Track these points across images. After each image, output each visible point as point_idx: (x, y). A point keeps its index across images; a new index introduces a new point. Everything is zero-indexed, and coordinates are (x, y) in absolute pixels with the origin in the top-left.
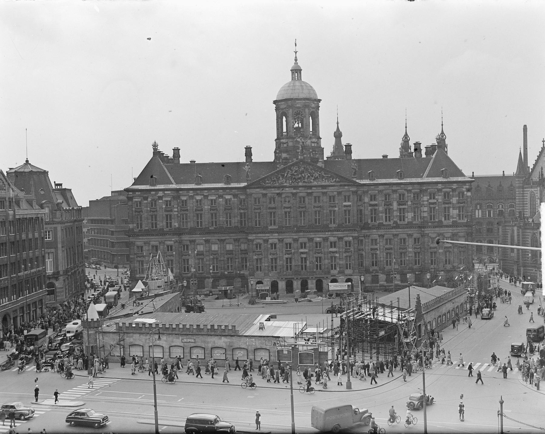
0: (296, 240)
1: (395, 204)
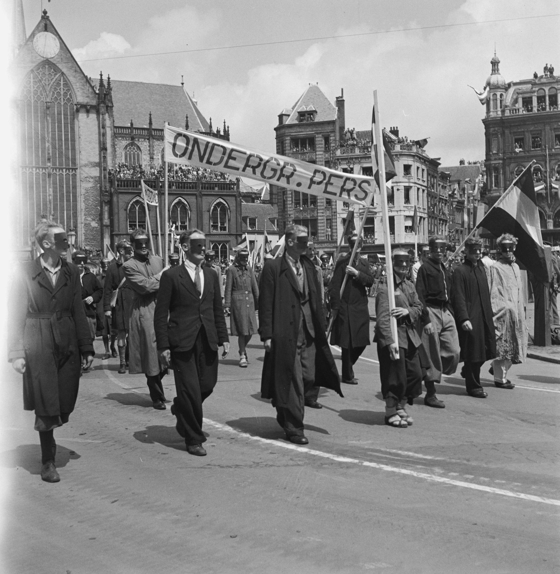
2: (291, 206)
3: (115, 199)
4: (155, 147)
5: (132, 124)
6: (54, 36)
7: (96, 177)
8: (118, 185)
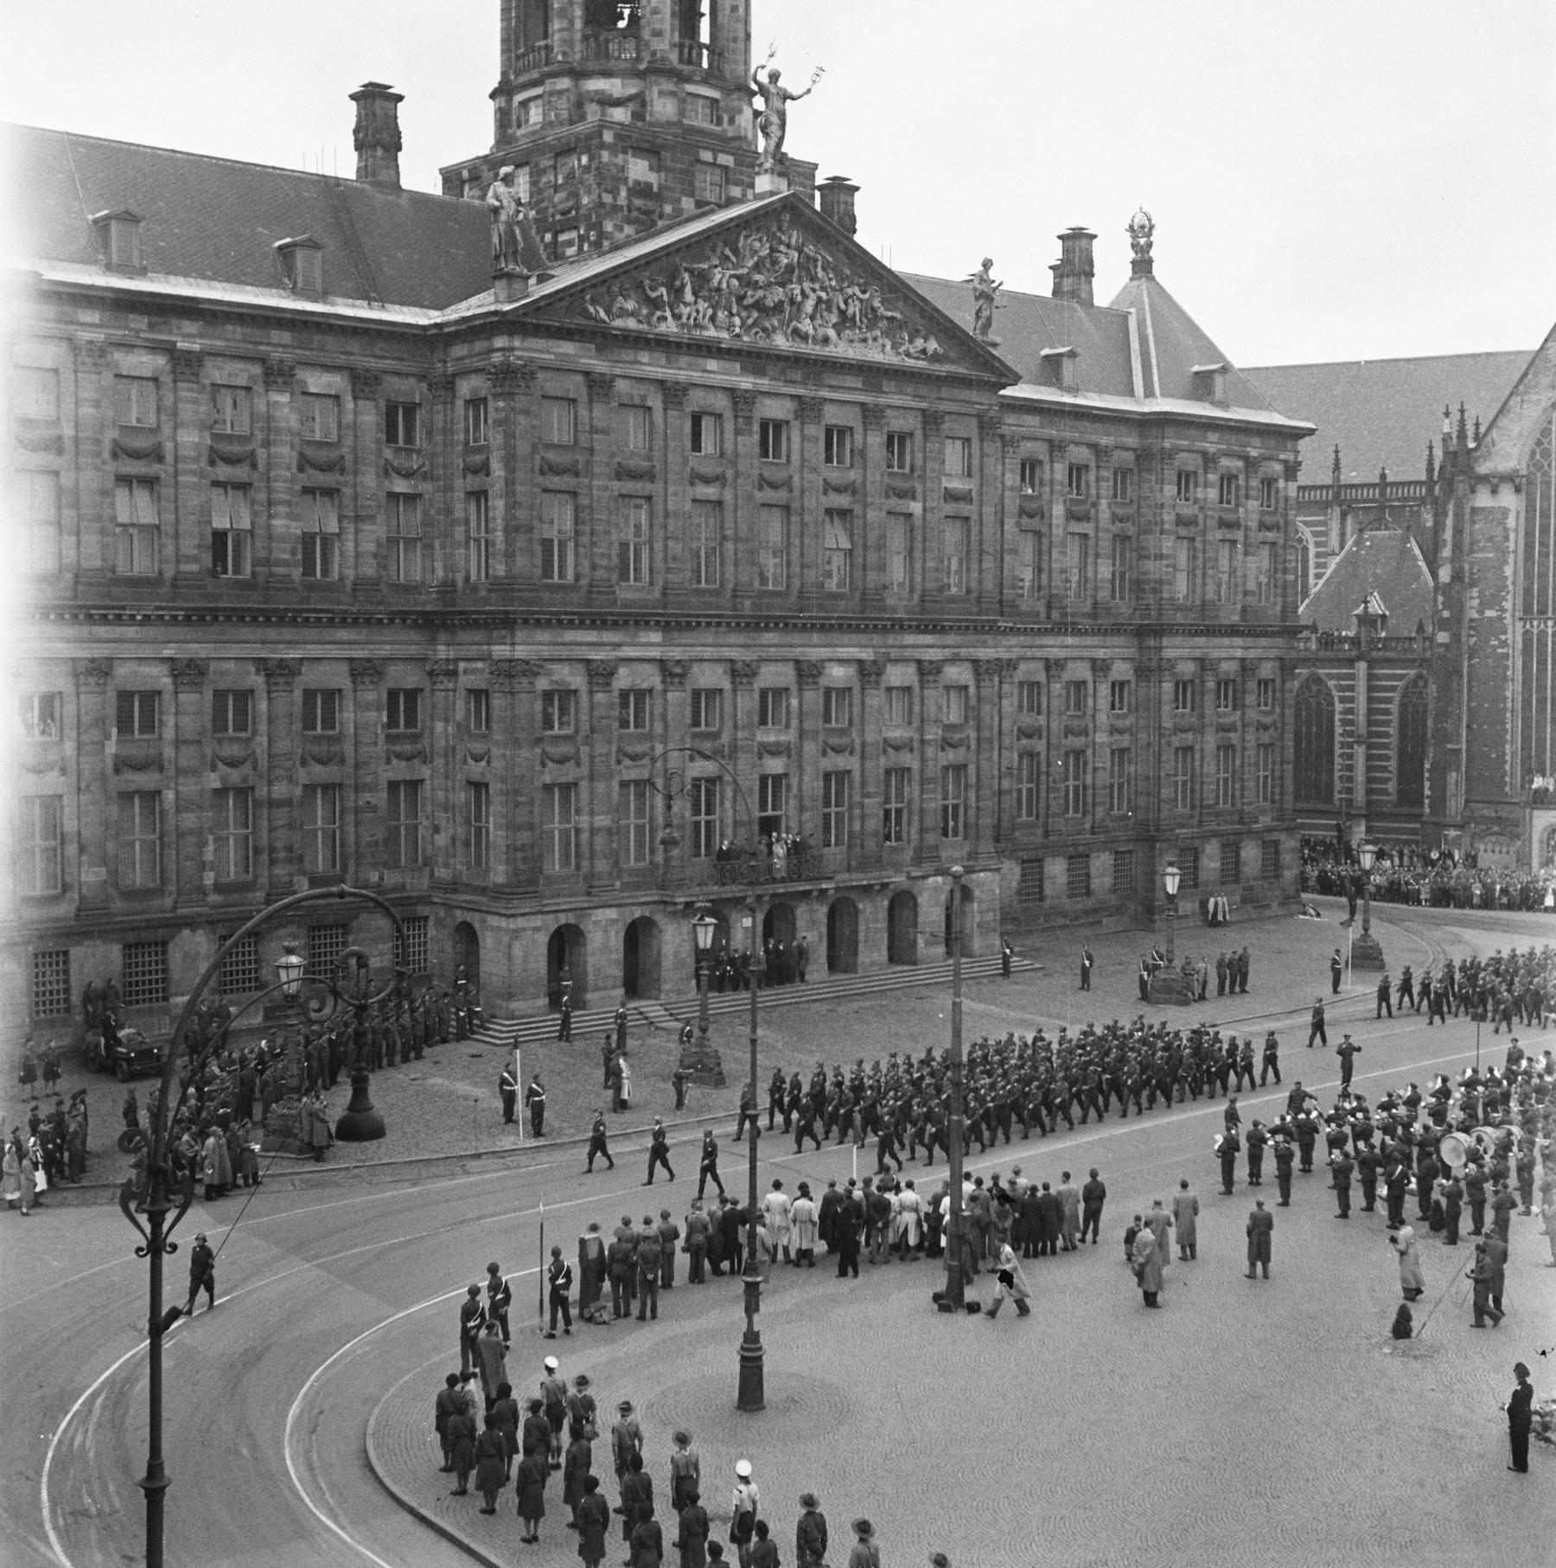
0: (741, 673)
1: (1058, 510)
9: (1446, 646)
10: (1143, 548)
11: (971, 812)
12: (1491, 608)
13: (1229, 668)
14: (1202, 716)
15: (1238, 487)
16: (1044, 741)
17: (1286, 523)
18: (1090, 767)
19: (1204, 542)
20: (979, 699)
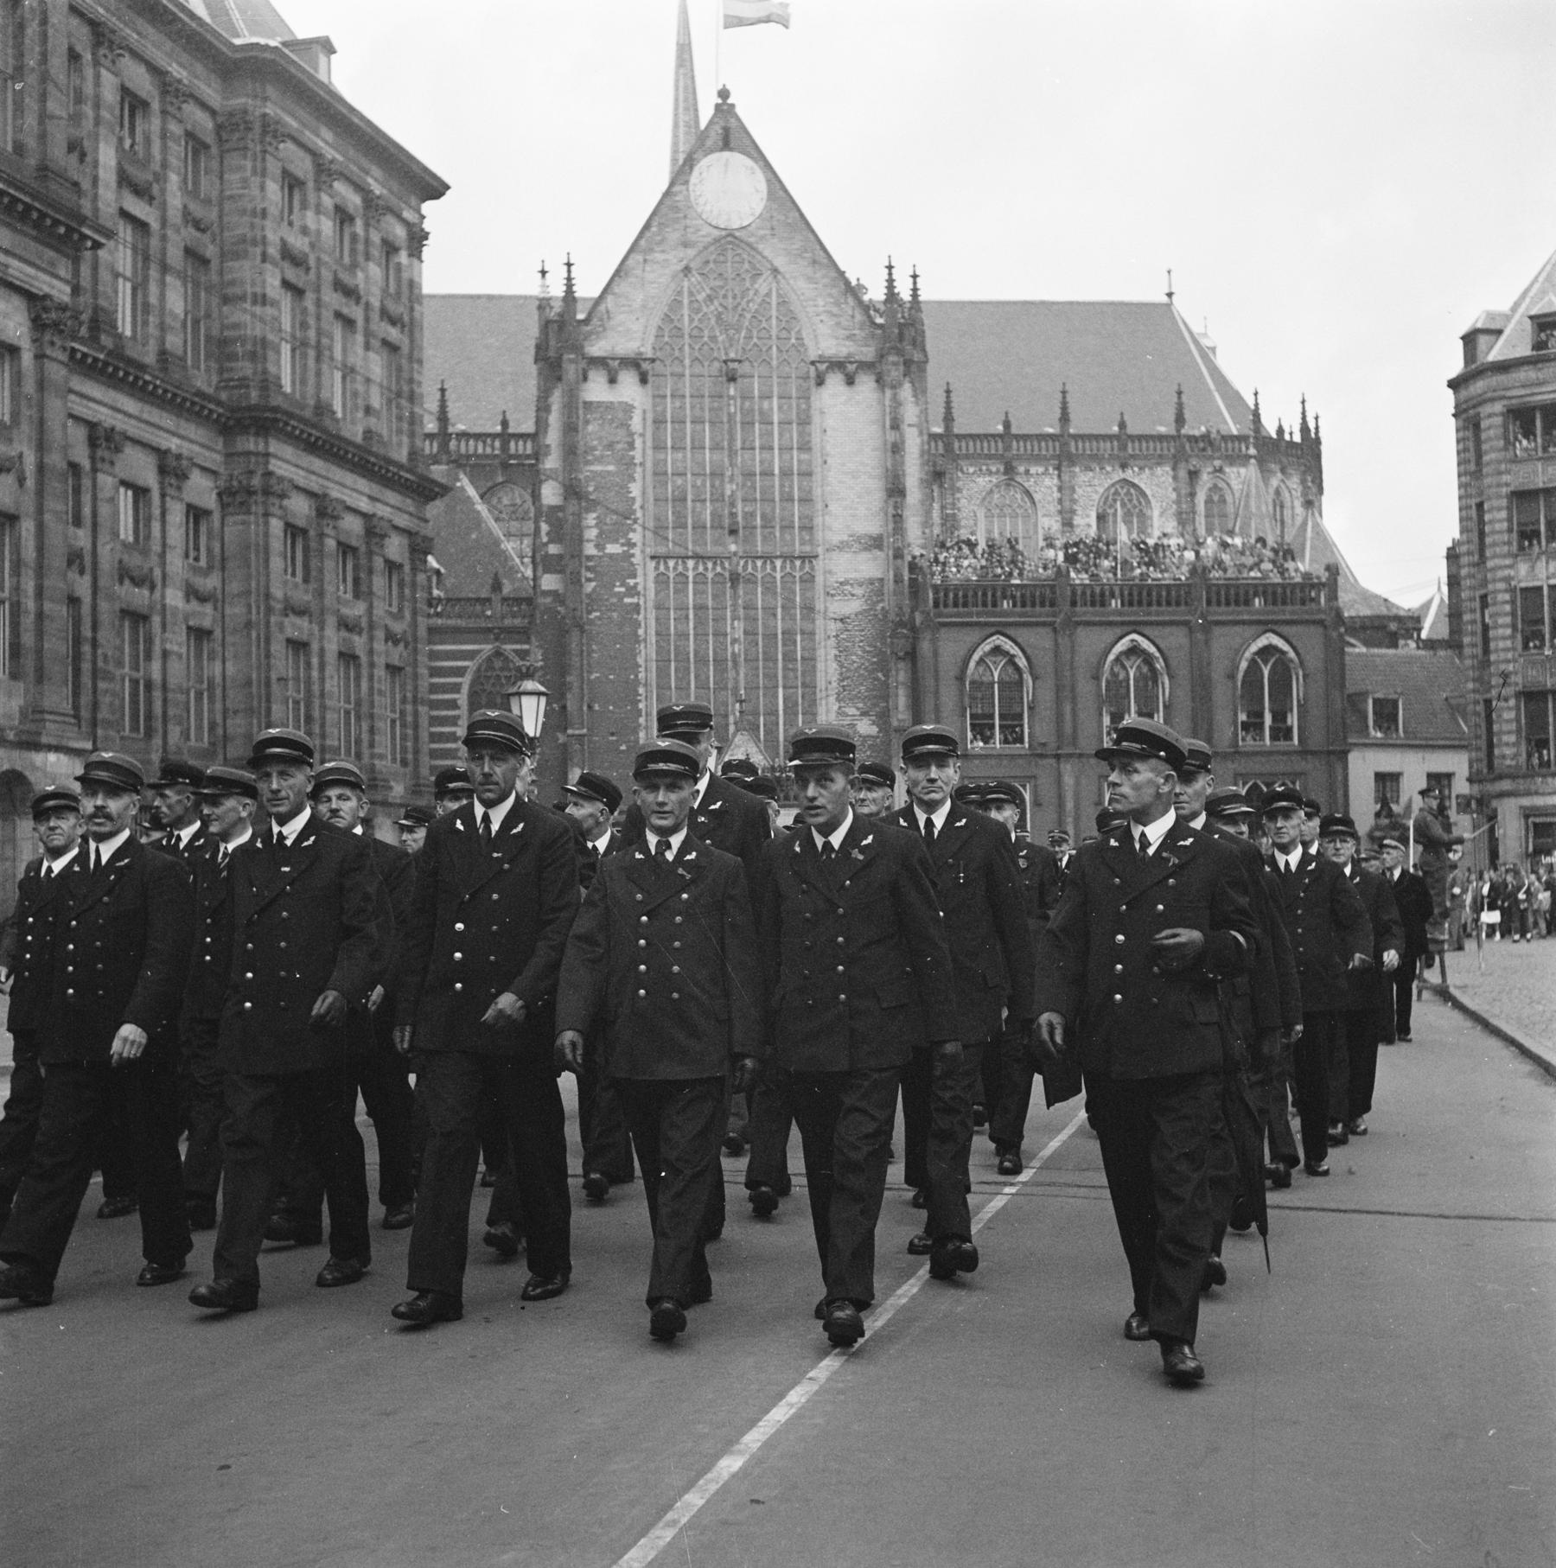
2: (1509, 643)
3: (925, 646)
4: (1079, 491)
5: (1007, 425)
6: (749, 162)
7: (871, 582)
8: (936, 604)
9: (554, 593)
10: (232, 283)
11: (28, 621)
12: (616, 541)
13: (352, 526)
14: (320, 593)
15: (354, 238)
16: (87, 578)
17: (412, 319)
18: (157, 649)
19: (318, 303)
20: (41, 385)
